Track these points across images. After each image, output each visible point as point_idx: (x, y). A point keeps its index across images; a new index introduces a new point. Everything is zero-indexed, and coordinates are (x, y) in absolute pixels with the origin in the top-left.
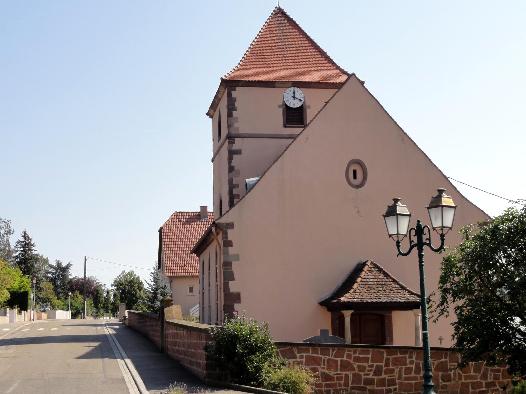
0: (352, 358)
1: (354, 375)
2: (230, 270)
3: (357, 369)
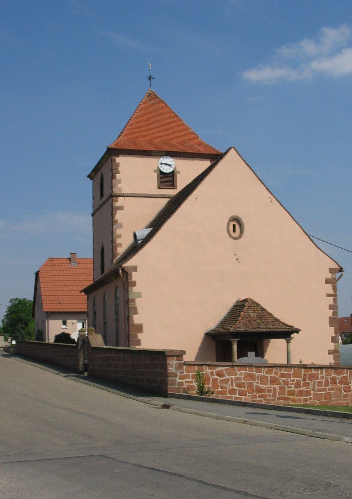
0: (279, 374)
1: (280, 388)
2: (134, 306)
3: (282, 383)
